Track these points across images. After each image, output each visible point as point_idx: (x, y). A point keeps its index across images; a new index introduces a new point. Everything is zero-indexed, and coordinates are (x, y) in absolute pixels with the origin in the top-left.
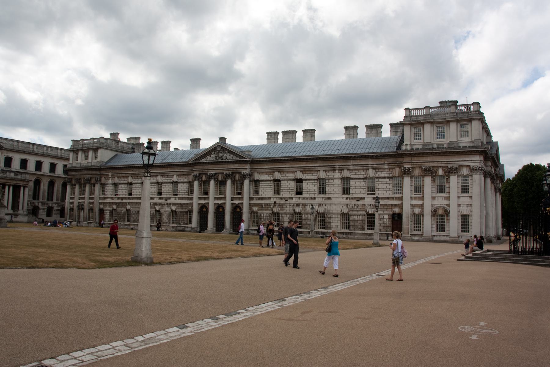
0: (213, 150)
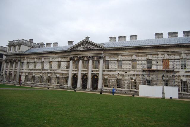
0: (82, 43)
